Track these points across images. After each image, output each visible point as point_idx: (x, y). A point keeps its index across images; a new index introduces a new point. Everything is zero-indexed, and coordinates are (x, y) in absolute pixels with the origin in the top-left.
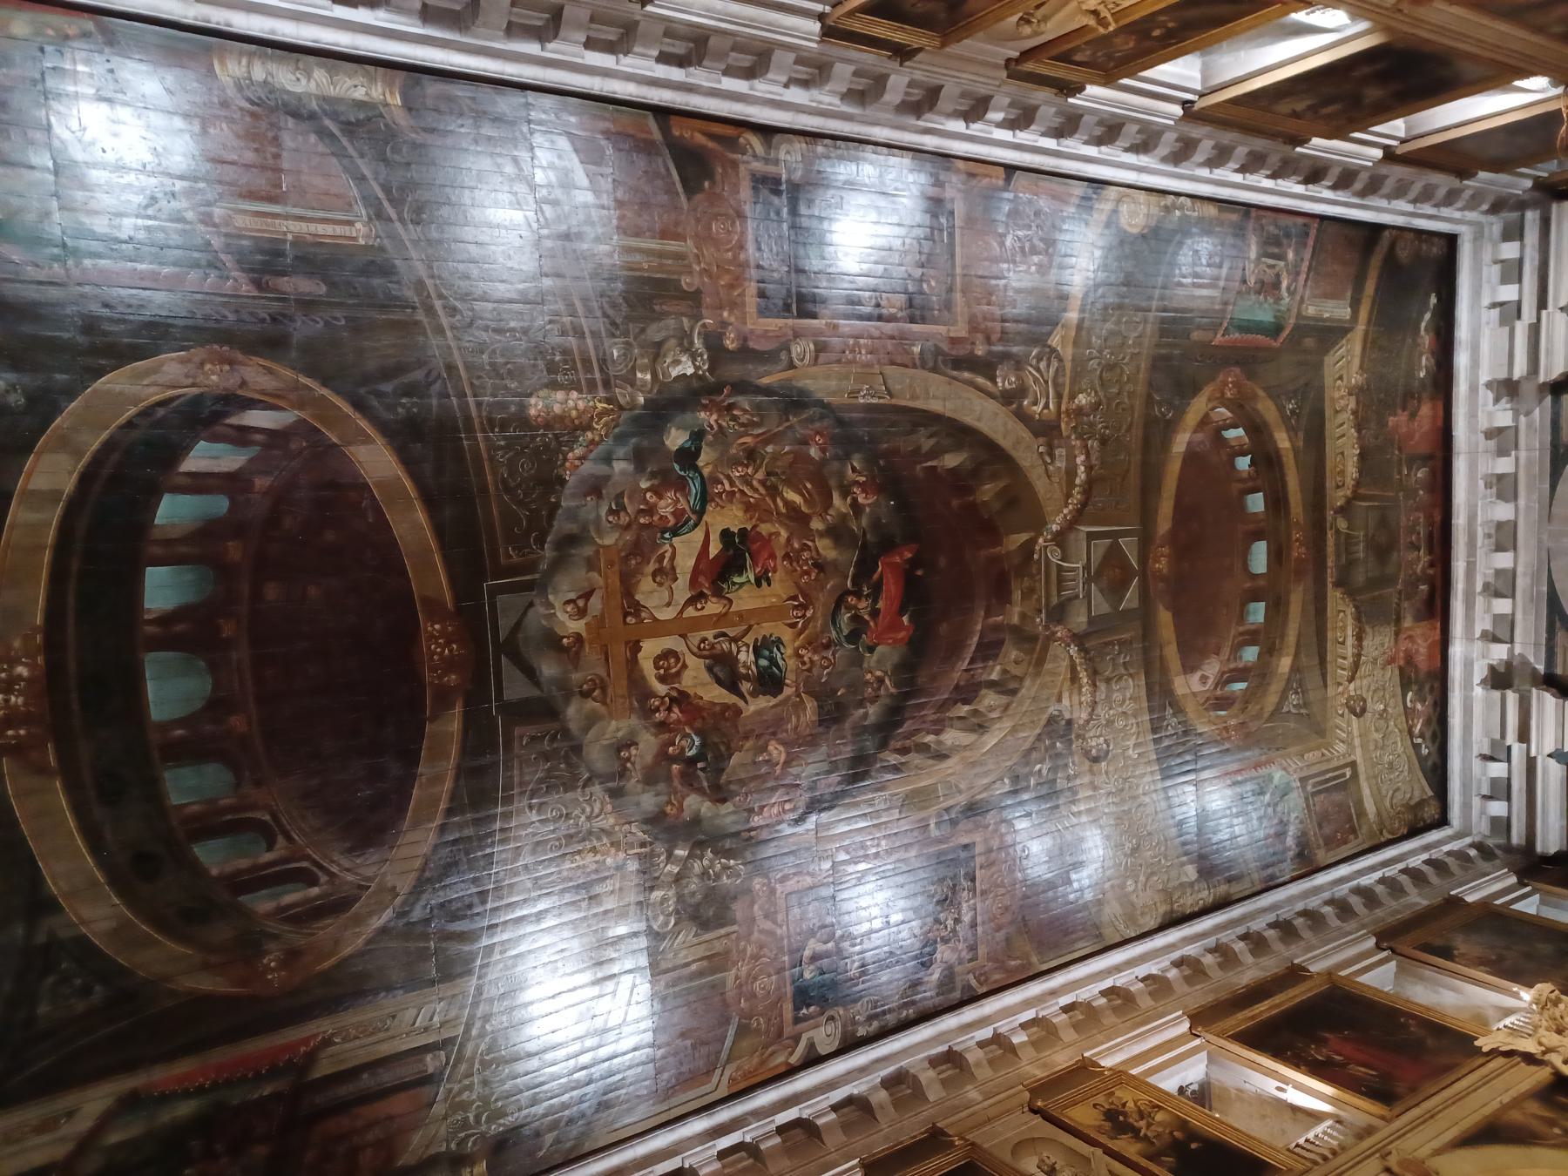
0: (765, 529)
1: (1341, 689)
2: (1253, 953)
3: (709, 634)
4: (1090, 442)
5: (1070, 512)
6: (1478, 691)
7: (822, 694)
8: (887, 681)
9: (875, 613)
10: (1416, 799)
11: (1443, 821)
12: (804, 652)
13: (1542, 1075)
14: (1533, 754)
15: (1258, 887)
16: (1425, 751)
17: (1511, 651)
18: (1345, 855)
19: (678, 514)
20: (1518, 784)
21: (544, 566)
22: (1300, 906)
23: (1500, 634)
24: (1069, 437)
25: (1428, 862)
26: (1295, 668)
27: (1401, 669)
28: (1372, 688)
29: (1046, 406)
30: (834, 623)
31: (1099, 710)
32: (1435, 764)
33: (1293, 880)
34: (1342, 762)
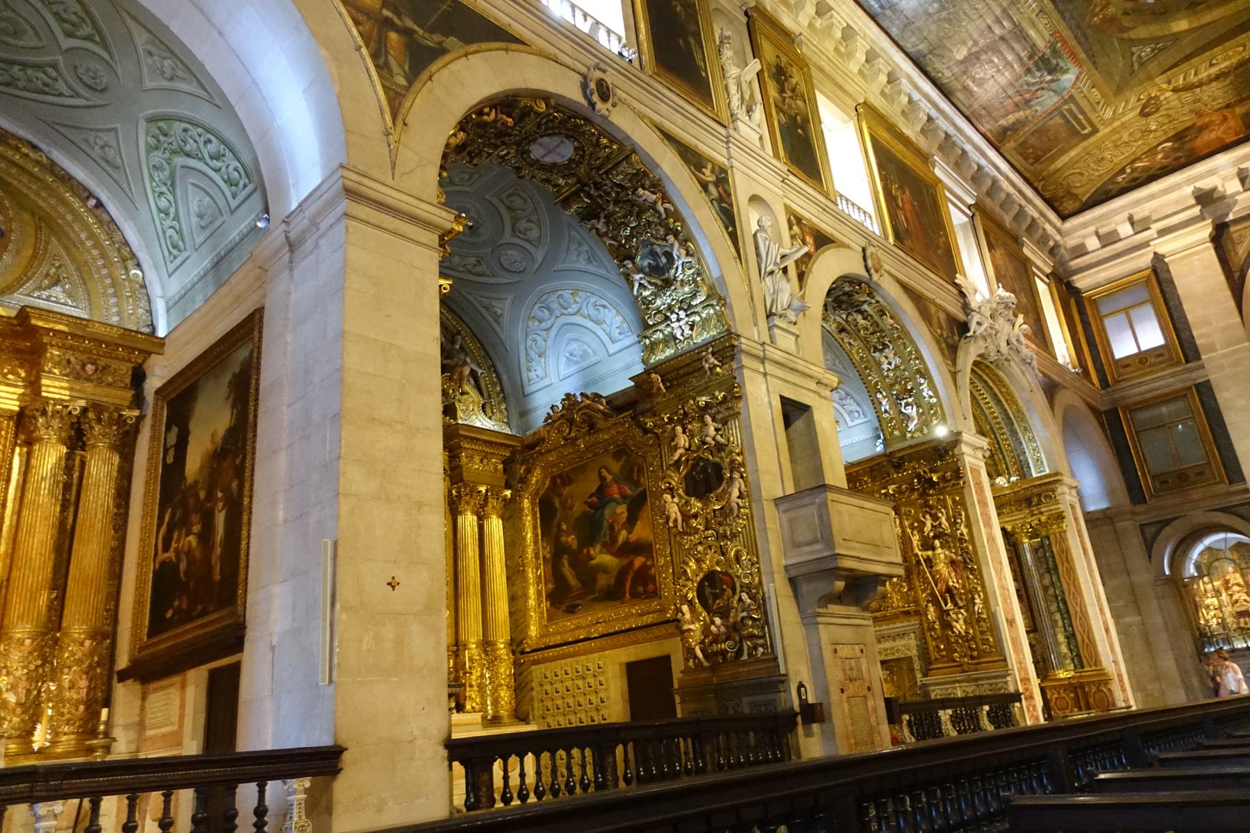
1: (1165, 86)
2: (922, 131)
6: (1189, 190)
10: (1075, 191)
11: (1064, 218)
13: (961, 316)
14: (1152, 243)
15: (967, 113)
16: (1120, 179)
17: (1238, 193)
18: (1015, 163)
20: (1118, 246)
22: (968, 147)
23: (1247, 181)
25: (1033, 220)
26: (1176, 37)
27: (1192, 126)
28: (1170, 112)
32: (1110, 191)
33: (984, 136)
34: (1095, 121)
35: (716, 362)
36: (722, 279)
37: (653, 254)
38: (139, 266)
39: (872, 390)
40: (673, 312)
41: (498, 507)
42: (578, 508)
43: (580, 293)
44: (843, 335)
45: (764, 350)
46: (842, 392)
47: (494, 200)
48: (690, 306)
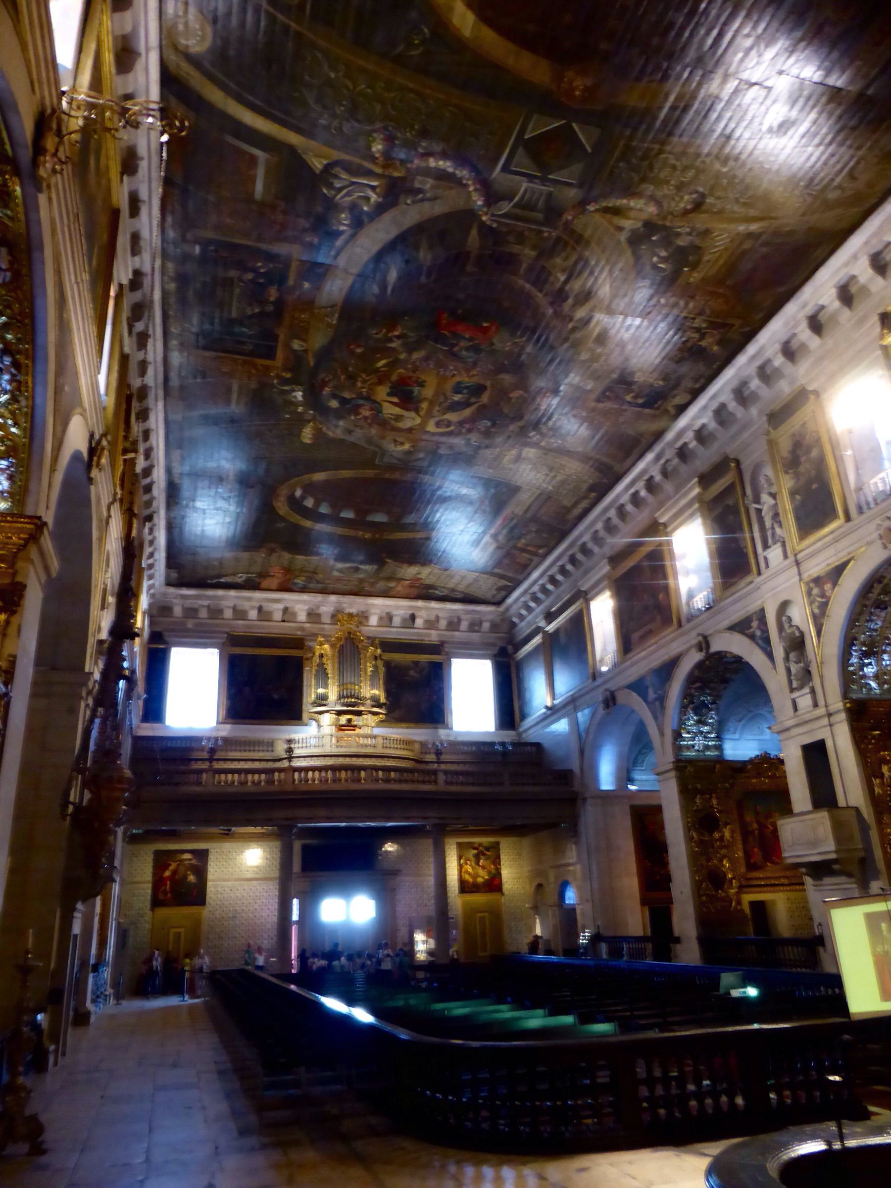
0: (394, 378)
3: (437, 408)
4: (421, 150)
5: (474, 184)
7: (501, 369)
8: (517, 340)
9: (470, 340)
12: (471, 374)
19: (371, 409)
21: (376, 449)
24: (408, 170)
29: (373, 188)
30: (462, 358)
31: (659, 194)
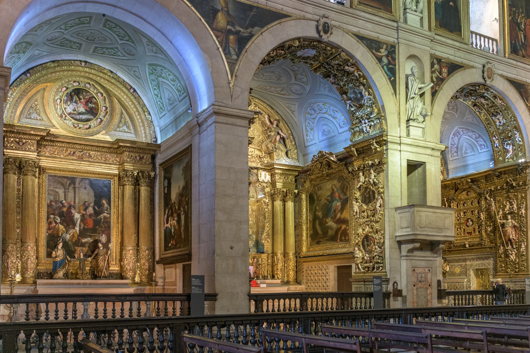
35: (377, 146)
36: (383, 106)
37: (355, 92)
38: (149, 114)
39: (491, 135)
40: (363, 119)
41: (292, 197)
42: (323, 201)
43: (326, 104)
44: (475, 107)
45: (400, 140)
46: (477, 135)
47: (286, 68)
48: (370, 118)
